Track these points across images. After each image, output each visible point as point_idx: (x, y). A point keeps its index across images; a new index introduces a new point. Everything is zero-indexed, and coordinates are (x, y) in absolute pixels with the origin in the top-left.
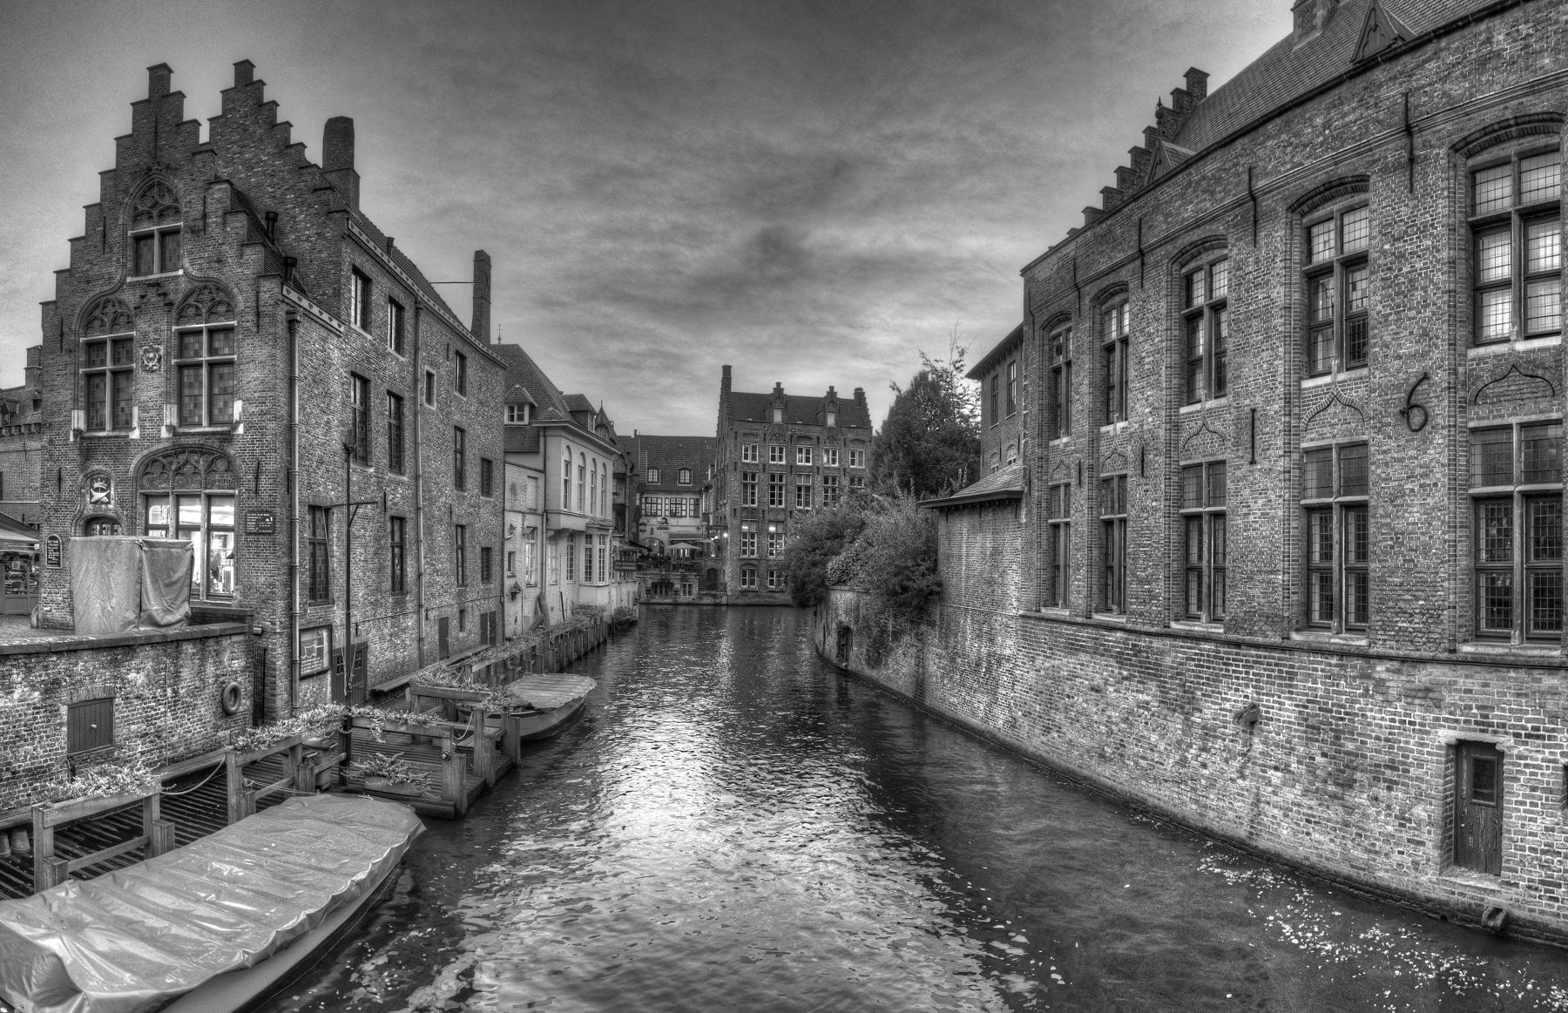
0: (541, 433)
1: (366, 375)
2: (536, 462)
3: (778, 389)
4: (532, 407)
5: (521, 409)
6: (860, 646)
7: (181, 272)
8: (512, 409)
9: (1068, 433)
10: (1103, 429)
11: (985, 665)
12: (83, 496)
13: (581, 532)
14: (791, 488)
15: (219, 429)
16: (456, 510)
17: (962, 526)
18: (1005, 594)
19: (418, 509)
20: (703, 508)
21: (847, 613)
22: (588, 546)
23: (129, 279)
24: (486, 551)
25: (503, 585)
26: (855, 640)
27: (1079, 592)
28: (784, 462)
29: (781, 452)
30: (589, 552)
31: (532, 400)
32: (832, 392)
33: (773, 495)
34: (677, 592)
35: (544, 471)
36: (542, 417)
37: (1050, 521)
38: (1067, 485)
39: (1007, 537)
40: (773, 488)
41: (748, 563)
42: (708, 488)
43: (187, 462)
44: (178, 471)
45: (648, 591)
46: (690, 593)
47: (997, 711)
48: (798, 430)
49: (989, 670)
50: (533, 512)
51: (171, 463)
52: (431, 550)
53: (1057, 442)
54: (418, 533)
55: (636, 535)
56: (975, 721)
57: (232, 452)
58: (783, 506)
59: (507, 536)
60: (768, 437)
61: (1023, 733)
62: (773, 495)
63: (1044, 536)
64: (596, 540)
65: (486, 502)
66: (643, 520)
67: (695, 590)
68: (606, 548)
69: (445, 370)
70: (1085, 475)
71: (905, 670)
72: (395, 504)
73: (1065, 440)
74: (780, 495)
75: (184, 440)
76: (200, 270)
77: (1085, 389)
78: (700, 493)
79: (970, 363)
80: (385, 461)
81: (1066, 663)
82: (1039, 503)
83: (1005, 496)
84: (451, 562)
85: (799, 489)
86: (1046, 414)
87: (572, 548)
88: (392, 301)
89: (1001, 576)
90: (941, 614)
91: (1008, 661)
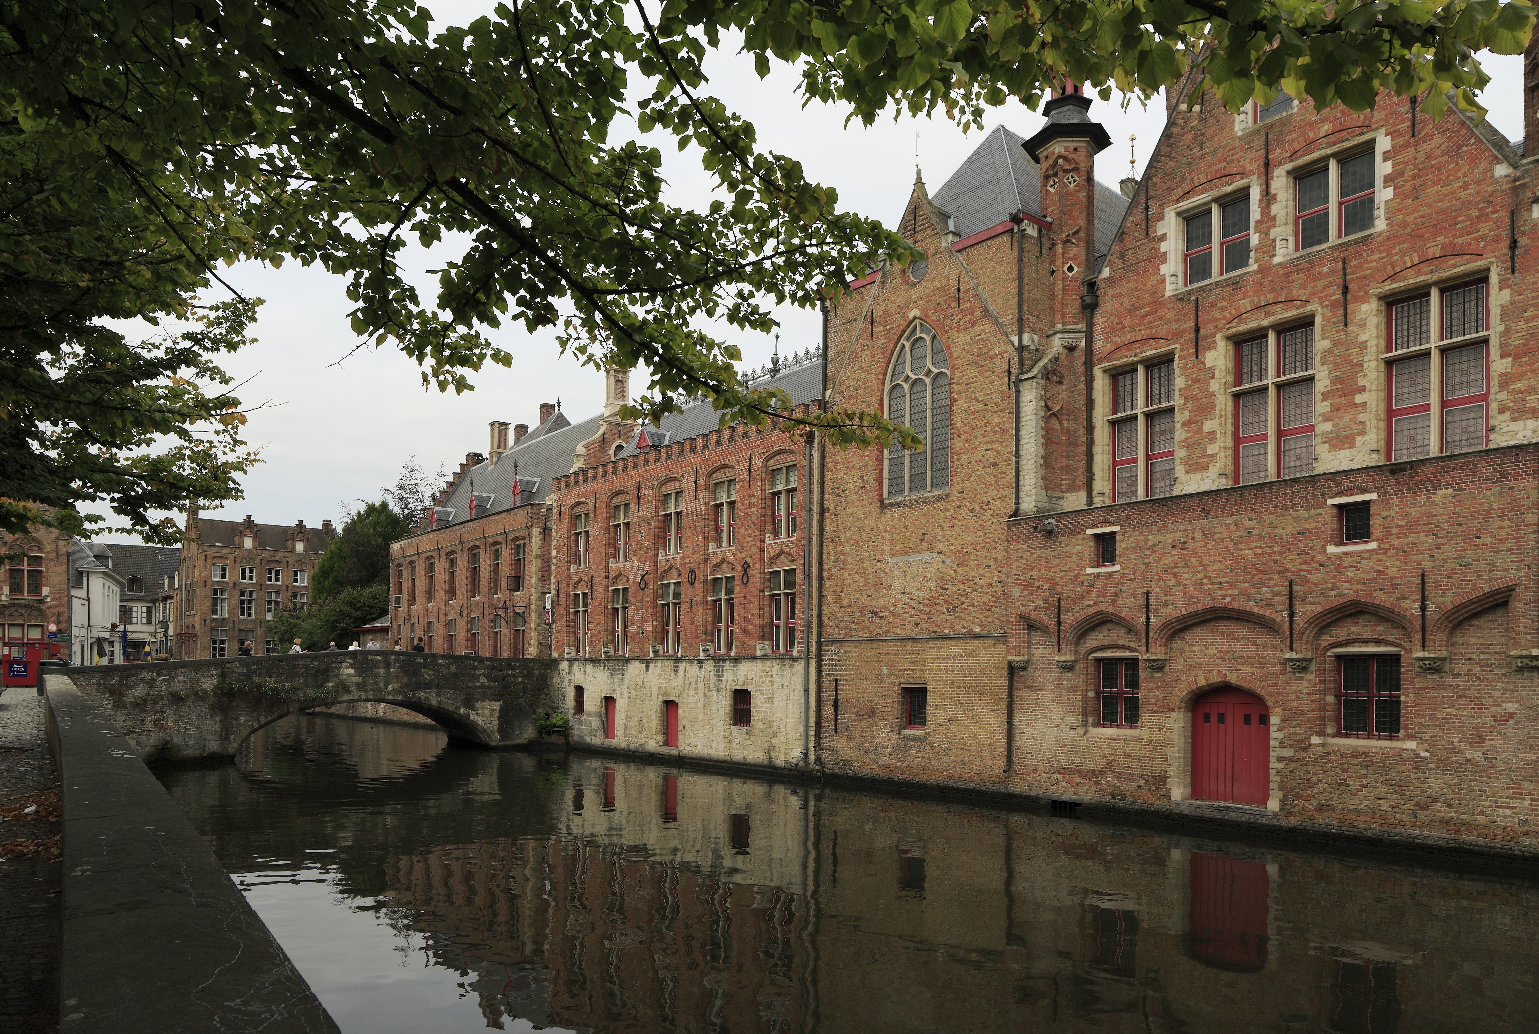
3: (249, 520)
14: (262, 602)
28: (254, 581)
29: (251, 571)
40: (243, 602)
58: (253, 617)
60: (238, 560)
74: (250, 608)
78: (154, 602)
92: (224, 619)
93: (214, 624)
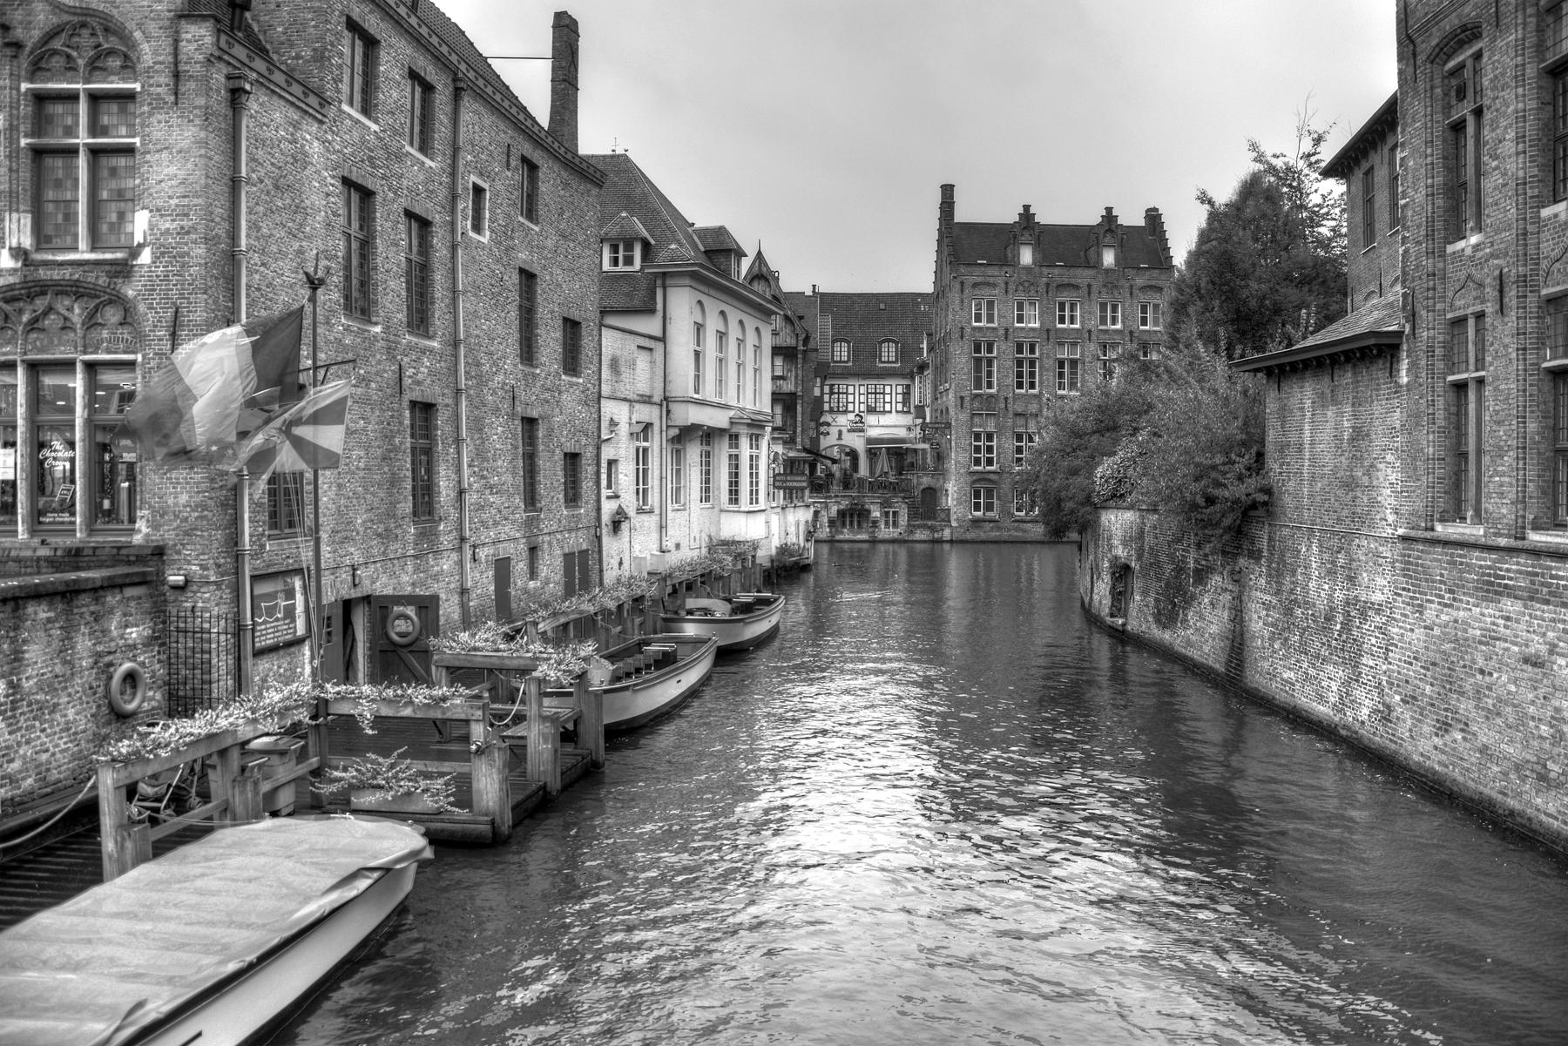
0: (659, 282)
1: (369, 184)
2: (651, 325)
3: (1027, 215)
4: (646, 246)
5: (629, 247)
6: (1145, 593)
8: (615, 249)
9: (1479, 228)
10: (1546, 212)
11: (1340, 618)
13: (722, 431)
14: (1049, 363)
15: (108, 256)
16: (522, 395)
17: (1304, 394)
18: (1374, 503)
19: (458, 391)
20: (915, 399)
21: (1125, 543)
22: (734, 451)
24: (572, 459)
25: (599, 509)
26: (1138, 584)
27: (1501, 495)
30: (735, 460)
31: (645, 234)
32: (1109, 216)
33: (1020, 375)
34: (875, 523)
35: (663, 339)
36: (662, 257)
37: (1450, 378)
38: (1480, 316)
39: (1377, 409)
40: (1020, 363)
41: (981, 478)
42: (922, 368)
43: (50, 310)
44: (33, 325)
45: (832, 523)
46: (895, 524)
47: (1359, 693)
48: (1058, 274)
49: (1346, 627)
50: (646, 400)
51: (20, 312)
52: (480, 454)
53: (1461, 244)
54: (458, 428)
55: (815, 441)
56: (1322, 710)
57: (130, 293)
59: (604, 437)
60: (1012, 287)
61: (1403, 731)
62: (1020, 375)
63: (1440, 403)
64: (744, 443)
65: (572, 385)
66: (827, 418)
67: (903, 520)
68: (763, 456)
69: (503, 185)
70: (1512, 293)
71: (1214, 629)
72: (418, 383)
73: (1474, 239)
74: (1032, 375)
75: (43, 274)
77: (1509, 147)
79: (1328, 153)
80: (401, 316)
81: (1478, 615)
82: (1430, 350)
83: (1372, 341)
84: (514, 474)
85: (1061, 364)
86: (1440, 202)
87: (708, 454)
88: (413, 75)
89: (1368, 474)
90: (1270, 539)
91: (1378, 612)
92: (992, 396)
93: (976, 405)
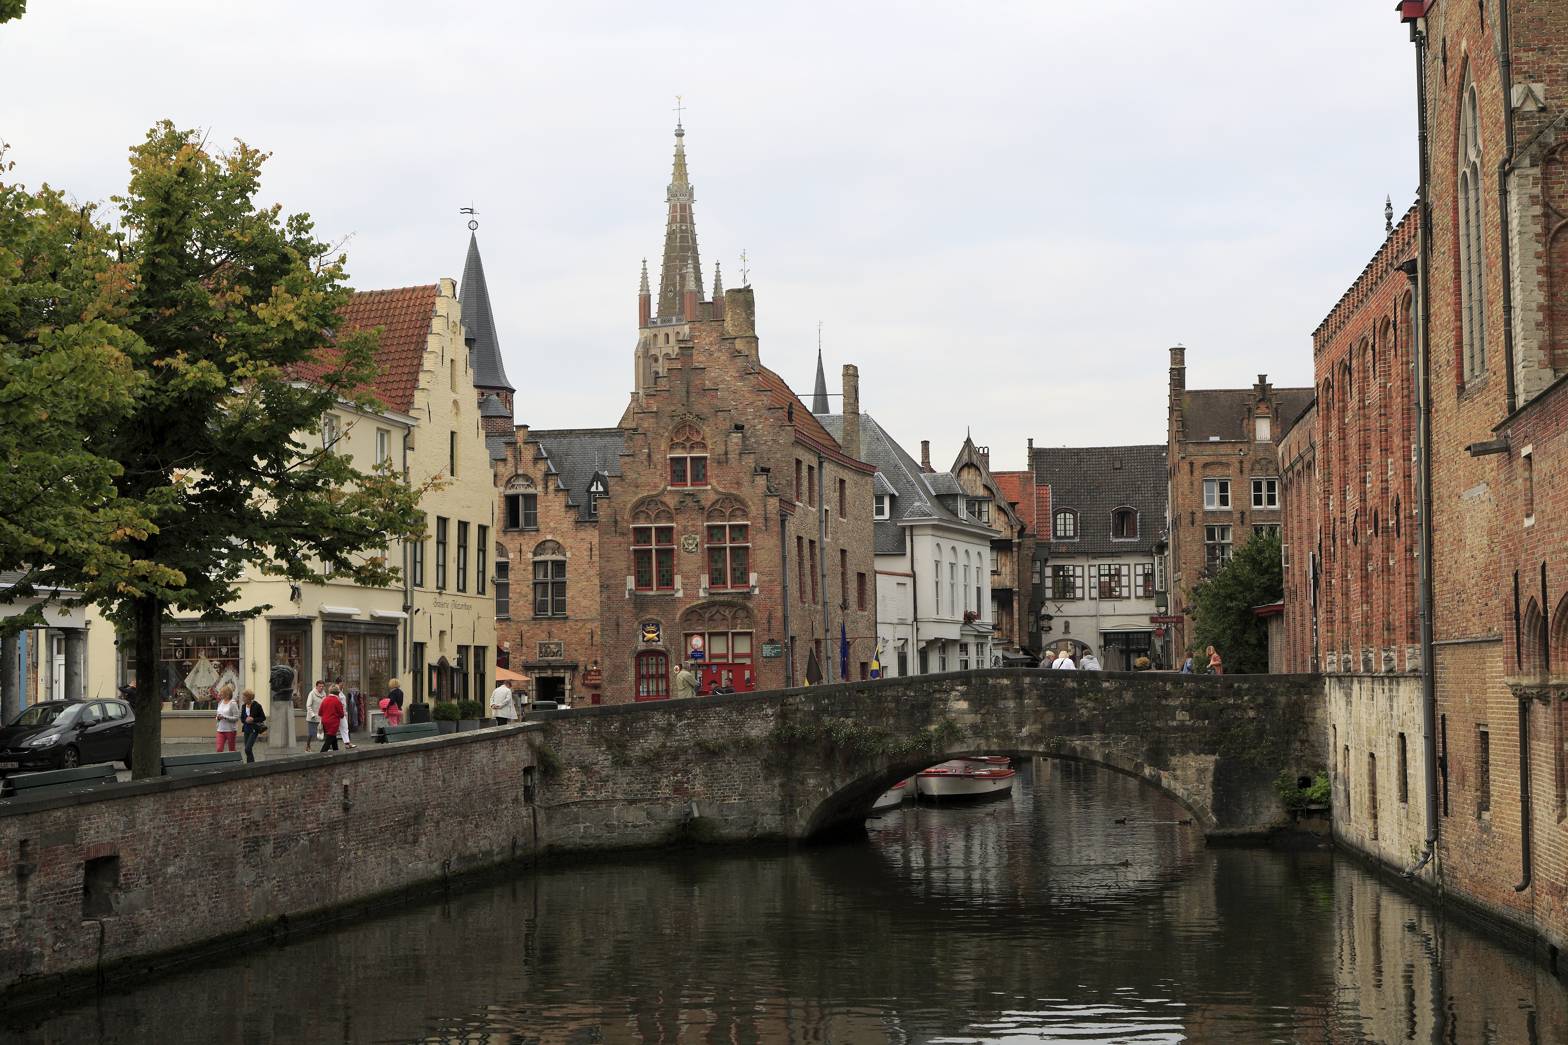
7: (709, 487)
12: (637, 636)
23: (669, 488)
75: (717, 598)
76: (725, 488)
